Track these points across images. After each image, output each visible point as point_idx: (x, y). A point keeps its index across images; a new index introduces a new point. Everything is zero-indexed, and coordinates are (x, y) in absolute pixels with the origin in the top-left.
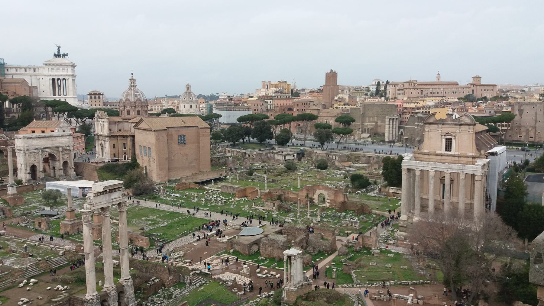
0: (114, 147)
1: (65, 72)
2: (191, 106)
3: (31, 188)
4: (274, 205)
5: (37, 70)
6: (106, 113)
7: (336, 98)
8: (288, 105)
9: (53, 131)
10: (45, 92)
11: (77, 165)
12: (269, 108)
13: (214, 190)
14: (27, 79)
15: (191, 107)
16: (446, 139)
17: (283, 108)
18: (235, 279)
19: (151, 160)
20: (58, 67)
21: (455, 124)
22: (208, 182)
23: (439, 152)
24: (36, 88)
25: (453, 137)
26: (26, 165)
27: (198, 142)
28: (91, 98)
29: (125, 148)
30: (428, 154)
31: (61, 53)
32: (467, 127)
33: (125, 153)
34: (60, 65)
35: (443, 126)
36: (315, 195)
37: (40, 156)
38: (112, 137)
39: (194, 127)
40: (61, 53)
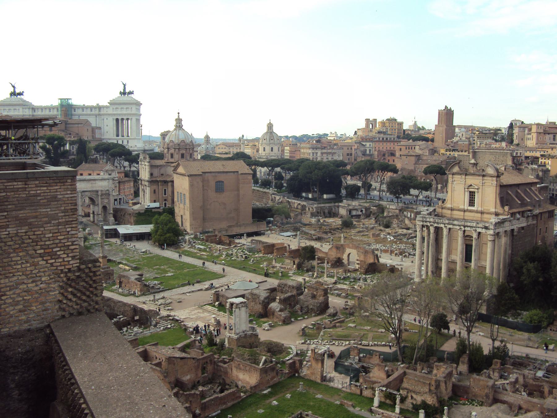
1: (129, 112)
2: (272, 148)
5: (102, 109)
8: (388, 149)
9: (99, 174)
10: (109, 134)
11: (116, 211)
12: (368, 152)
13: (244, 245)
15: (272, 150)
16: (470, 192)
17: (382, 153)
19: (186, 208)
20: (122, 106)
21: (479, 175)
22: (241, 236)
23: (462, 207)
24: (100, 128)
25: (476, 190)
29: (165, 194)
30: (452, 209)
31: (127, 91)
32: (490, 178)
33: (165, 200)
35: (467, 177)
36: (344, 255)
38: (152, 182)
39: (234, 172)
40: (127, 91)
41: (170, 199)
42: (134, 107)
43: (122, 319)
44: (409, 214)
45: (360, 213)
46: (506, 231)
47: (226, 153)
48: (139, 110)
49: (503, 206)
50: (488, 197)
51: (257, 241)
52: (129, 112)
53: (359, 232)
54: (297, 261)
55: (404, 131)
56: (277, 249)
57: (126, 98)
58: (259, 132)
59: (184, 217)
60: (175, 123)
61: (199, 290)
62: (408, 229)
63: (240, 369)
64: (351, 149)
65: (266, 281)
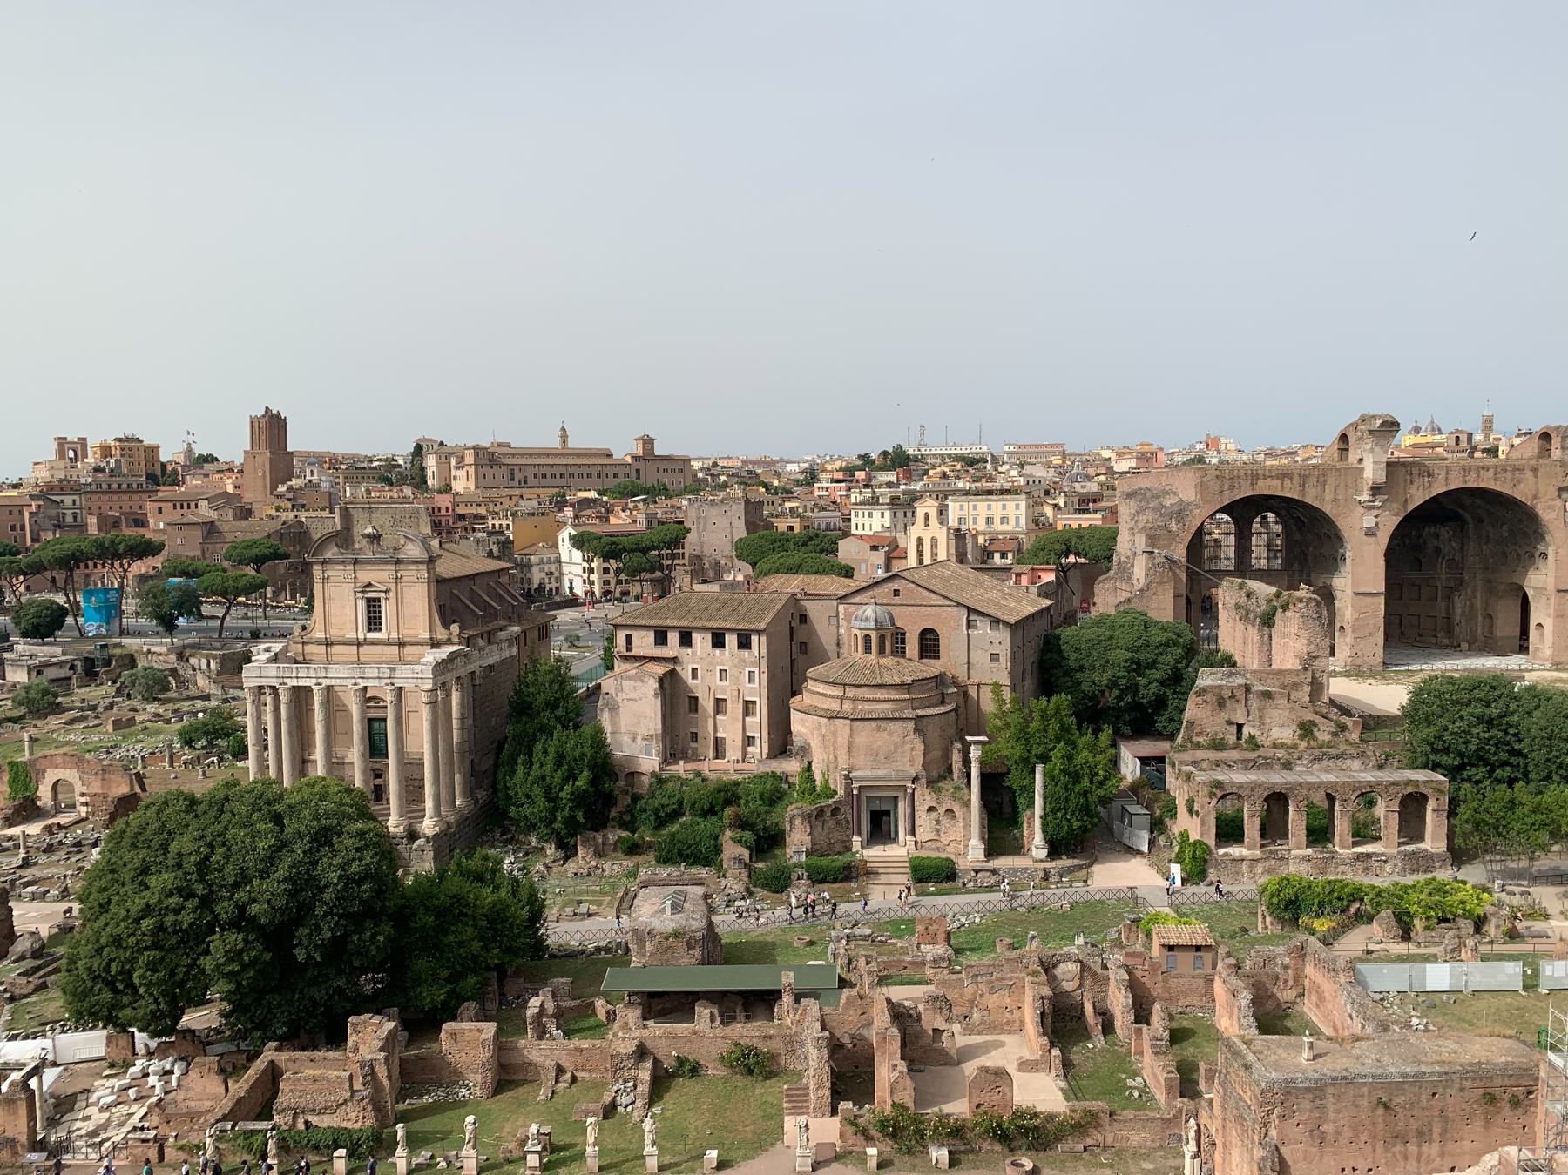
7: (282, 489)
8: (126, 509)
12: (69, 519)
16: (369, 600)
23: (351, 635)
44: (204, 661)
45: (65, 672)
46: (458, 678)
49: (446, 626)
50: (411, 607)
55: (164, 466)
62: (207, 697)
64: (21, 512)
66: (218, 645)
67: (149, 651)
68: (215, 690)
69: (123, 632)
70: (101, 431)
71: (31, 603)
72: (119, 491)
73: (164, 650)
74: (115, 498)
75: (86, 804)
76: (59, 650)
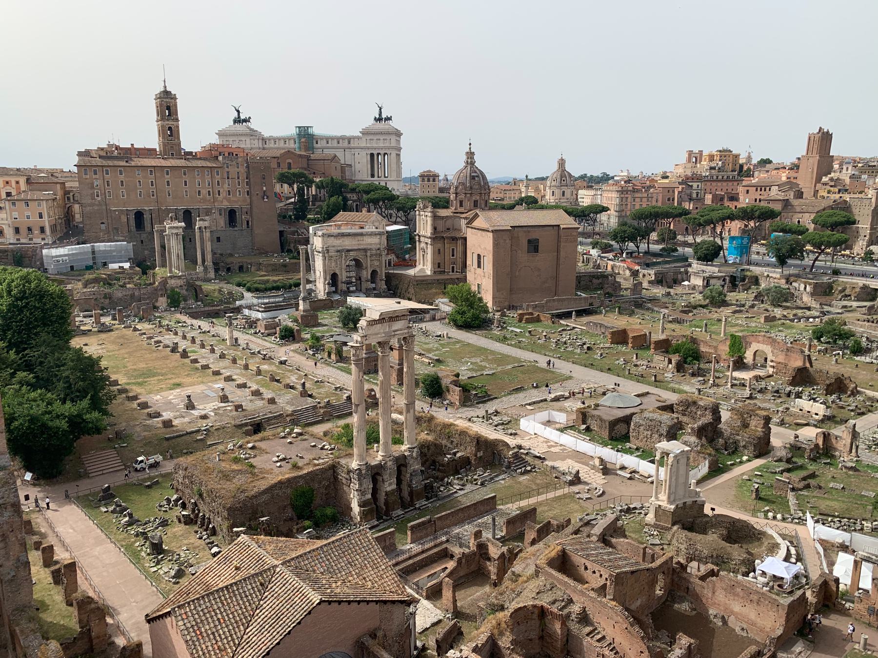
0: (439, 253)
2: (564, 192)
3: (327, 305)
4: (670, 362)
6: (430, 204)
7: (825, 179)
10: (361, 173)
12: (694, 196)
13: (574, 328)
14: (340, 154)
15: (563, 195)
18: (578, 472)
20: (378, 137)
22: (567, 315)
26: (325, 272)
27: (558, 251)
28: (423, 180)
31: (384, 116)
34: (381, 133)
37: (343, 262)
39: (553, 226)
40: (384, 116)
41: (459, 261)
42: (393, 138)
43: (458, 455)
44: (802, 286)
47: (502, 199)
48: (398, 142)
51: (595, 323)
52: (387, 145)
53: (735, 312)
54: (675, 358)
56: (634, 337)
57: (382, 126)
58: (550, 169)
59: (483, 287)
60: (465, 158)
61: (542, 401)
62: (809, 309)
63: (736, 595)
64: (674, 191)
65: (648, 393)
66: (811, 276)
67: (768, 276)
68: (814, 304)
69: (749, 263)
70: (710, 148)
71: (704, 242)
72: (722, 180)
73: (778, 276)
74: (719, 184)
75: (773, 367)
76: (717, 269)
